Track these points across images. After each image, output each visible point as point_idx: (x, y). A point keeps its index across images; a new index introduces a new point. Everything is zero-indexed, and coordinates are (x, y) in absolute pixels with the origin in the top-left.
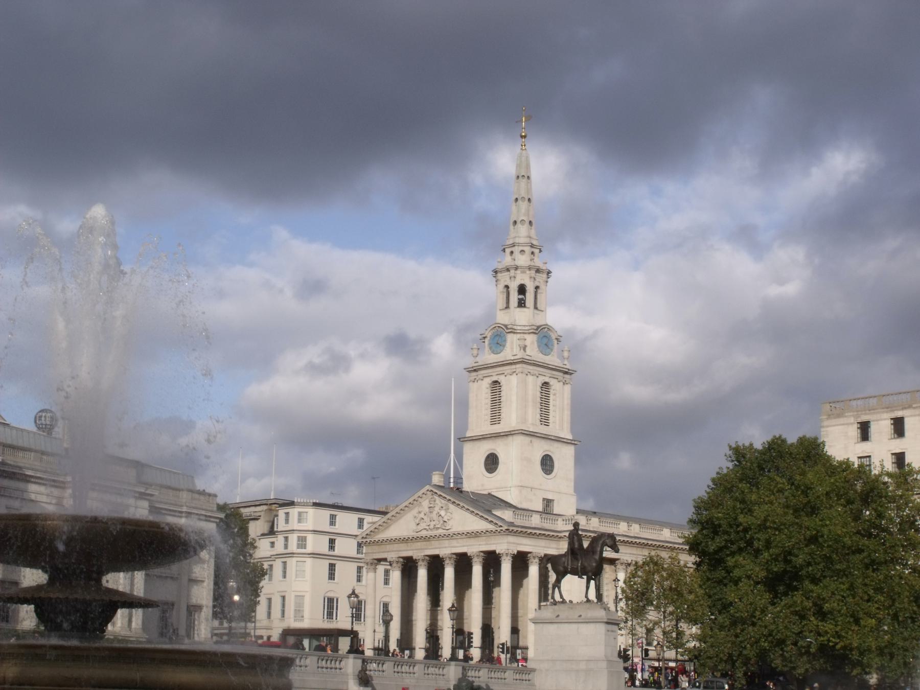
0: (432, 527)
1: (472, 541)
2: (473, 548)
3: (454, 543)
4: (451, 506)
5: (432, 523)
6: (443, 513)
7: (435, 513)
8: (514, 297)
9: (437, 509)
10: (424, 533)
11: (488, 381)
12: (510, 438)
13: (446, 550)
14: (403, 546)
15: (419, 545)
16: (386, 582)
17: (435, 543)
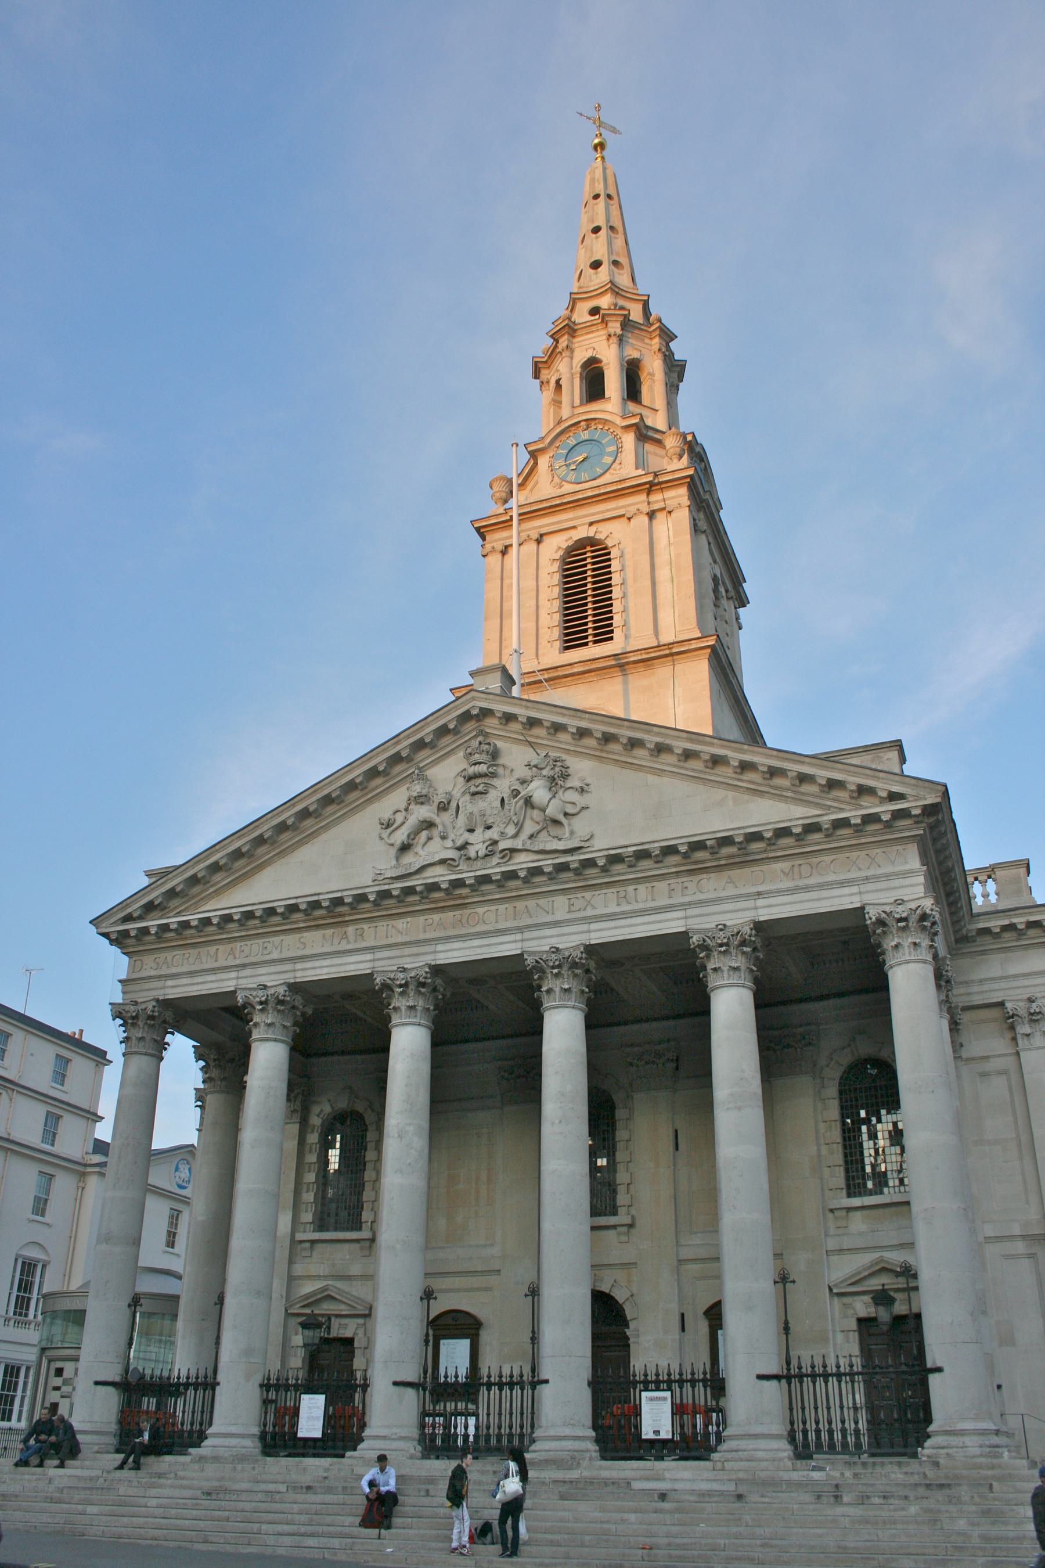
0: (478, 847)
1: (711, 885)
2: (719, 909)
3: (604, 902)
4: (581, 768)
5: (478, 842)
6: (539, 791)
7: (494, 796)
8: (614, 383)
9: (503, 786)
10: (441, 875)
11: (555, 547)
12: (663, 672)
13: (558, 929)
14: (315, 941)
15: (404, 928)
16: (40, 1206)
17: (490, 914)
